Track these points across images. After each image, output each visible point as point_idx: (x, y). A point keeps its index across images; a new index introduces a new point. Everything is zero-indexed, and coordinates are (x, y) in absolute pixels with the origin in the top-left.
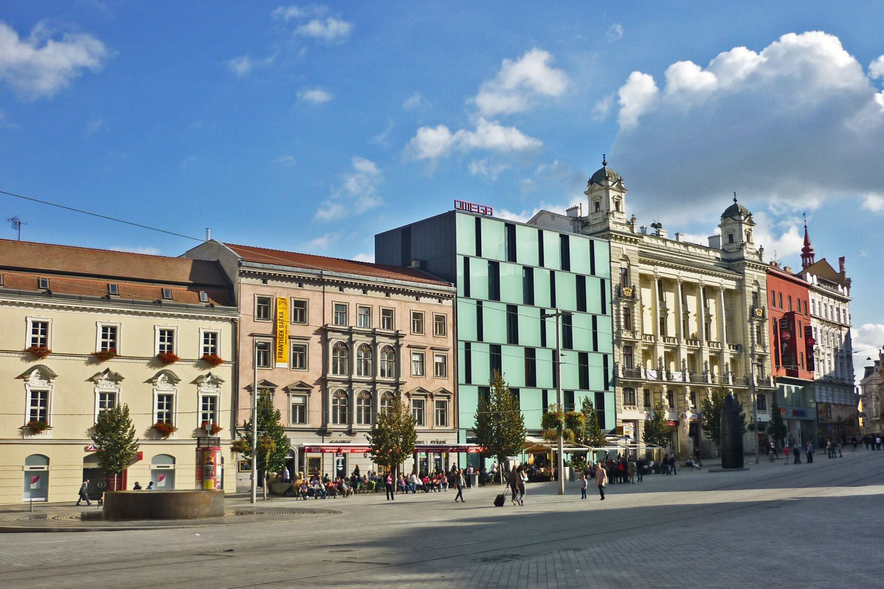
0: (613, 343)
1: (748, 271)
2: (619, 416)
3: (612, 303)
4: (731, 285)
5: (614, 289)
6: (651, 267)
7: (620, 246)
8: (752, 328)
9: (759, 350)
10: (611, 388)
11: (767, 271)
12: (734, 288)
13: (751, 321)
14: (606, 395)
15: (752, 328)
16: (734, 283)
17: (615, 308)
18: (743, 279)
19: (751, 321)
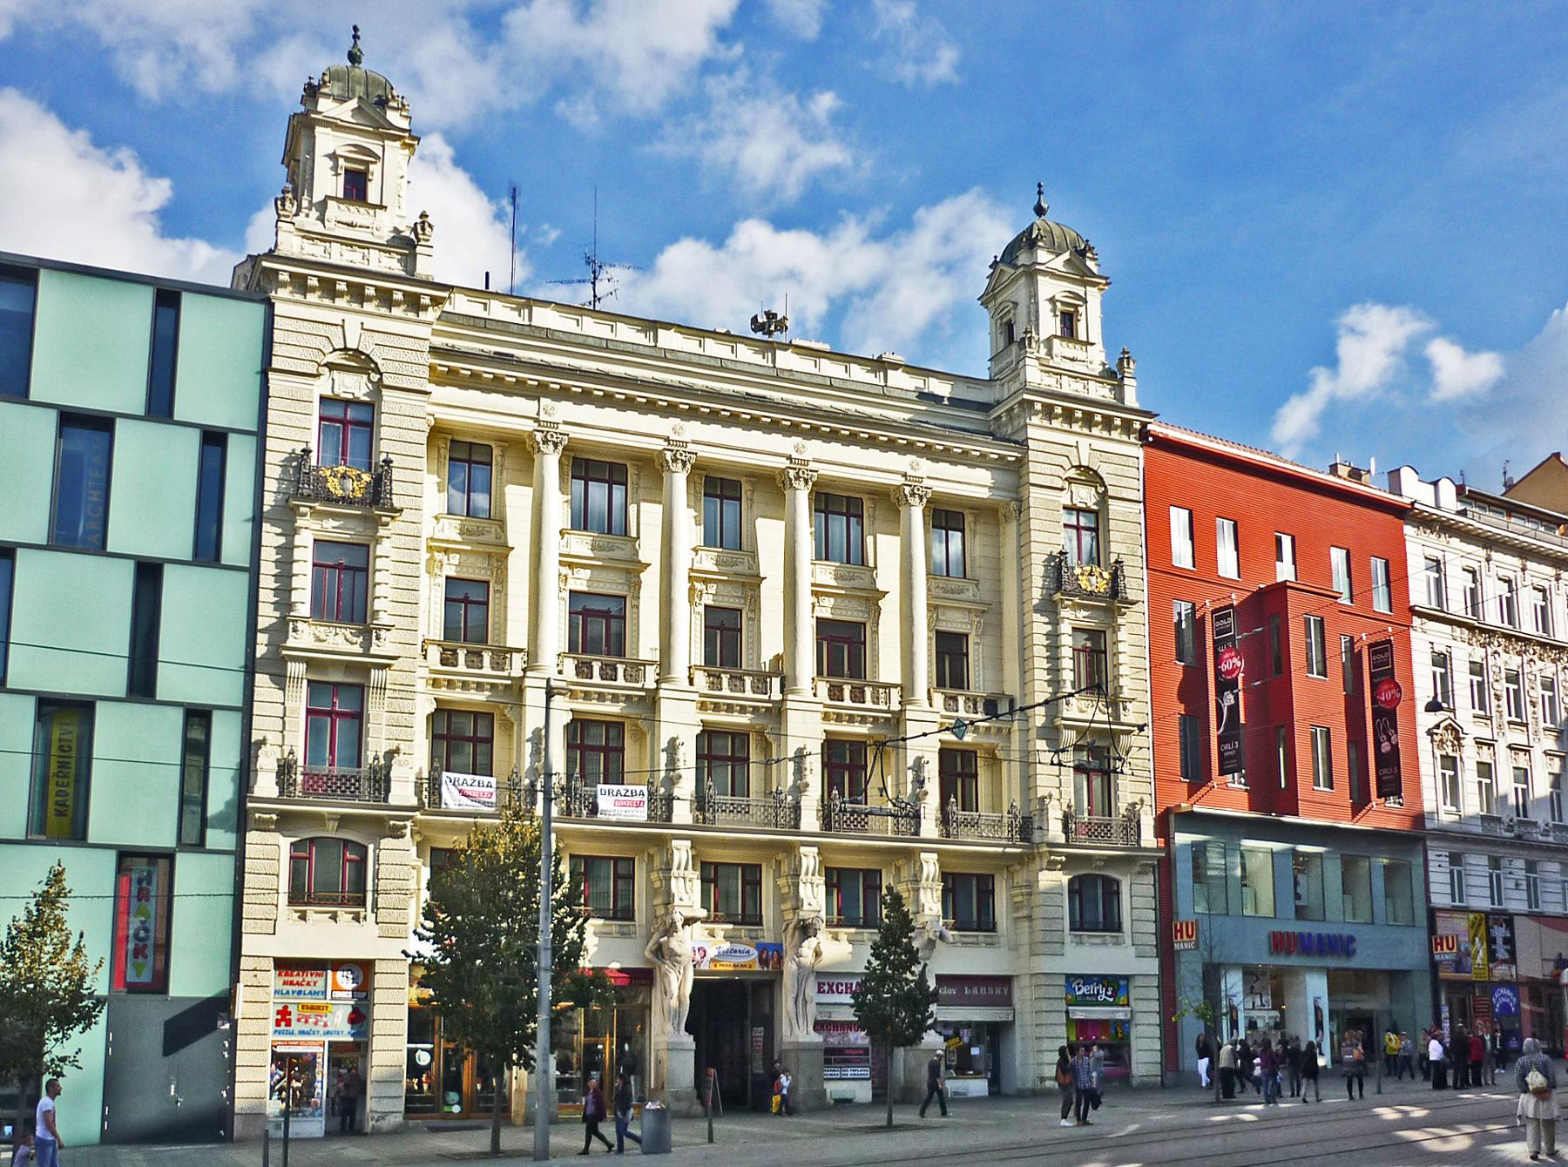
0: (251, 668)
1: (1038, 431)
2: (249, 945)
3: (258, 520)
4: (975, 483)
5: (273, 471)
6: (526, 406)
7: (336, 317)
8: (1054, 636)
9: (1081, 710)
10: (218, 838)
11: (1144, 434)
12: (984, 493)
13: (1049, 608)
14: (186, 865)
15: (1054, 636)
16: (984, 476)
17: (272, 537)
18: (1021, 463)
19: (1049, 608)
